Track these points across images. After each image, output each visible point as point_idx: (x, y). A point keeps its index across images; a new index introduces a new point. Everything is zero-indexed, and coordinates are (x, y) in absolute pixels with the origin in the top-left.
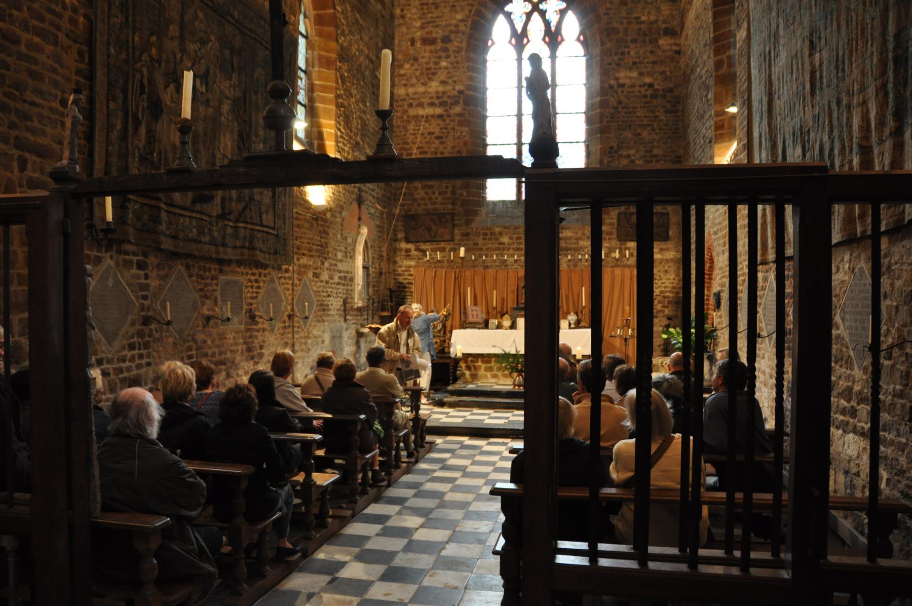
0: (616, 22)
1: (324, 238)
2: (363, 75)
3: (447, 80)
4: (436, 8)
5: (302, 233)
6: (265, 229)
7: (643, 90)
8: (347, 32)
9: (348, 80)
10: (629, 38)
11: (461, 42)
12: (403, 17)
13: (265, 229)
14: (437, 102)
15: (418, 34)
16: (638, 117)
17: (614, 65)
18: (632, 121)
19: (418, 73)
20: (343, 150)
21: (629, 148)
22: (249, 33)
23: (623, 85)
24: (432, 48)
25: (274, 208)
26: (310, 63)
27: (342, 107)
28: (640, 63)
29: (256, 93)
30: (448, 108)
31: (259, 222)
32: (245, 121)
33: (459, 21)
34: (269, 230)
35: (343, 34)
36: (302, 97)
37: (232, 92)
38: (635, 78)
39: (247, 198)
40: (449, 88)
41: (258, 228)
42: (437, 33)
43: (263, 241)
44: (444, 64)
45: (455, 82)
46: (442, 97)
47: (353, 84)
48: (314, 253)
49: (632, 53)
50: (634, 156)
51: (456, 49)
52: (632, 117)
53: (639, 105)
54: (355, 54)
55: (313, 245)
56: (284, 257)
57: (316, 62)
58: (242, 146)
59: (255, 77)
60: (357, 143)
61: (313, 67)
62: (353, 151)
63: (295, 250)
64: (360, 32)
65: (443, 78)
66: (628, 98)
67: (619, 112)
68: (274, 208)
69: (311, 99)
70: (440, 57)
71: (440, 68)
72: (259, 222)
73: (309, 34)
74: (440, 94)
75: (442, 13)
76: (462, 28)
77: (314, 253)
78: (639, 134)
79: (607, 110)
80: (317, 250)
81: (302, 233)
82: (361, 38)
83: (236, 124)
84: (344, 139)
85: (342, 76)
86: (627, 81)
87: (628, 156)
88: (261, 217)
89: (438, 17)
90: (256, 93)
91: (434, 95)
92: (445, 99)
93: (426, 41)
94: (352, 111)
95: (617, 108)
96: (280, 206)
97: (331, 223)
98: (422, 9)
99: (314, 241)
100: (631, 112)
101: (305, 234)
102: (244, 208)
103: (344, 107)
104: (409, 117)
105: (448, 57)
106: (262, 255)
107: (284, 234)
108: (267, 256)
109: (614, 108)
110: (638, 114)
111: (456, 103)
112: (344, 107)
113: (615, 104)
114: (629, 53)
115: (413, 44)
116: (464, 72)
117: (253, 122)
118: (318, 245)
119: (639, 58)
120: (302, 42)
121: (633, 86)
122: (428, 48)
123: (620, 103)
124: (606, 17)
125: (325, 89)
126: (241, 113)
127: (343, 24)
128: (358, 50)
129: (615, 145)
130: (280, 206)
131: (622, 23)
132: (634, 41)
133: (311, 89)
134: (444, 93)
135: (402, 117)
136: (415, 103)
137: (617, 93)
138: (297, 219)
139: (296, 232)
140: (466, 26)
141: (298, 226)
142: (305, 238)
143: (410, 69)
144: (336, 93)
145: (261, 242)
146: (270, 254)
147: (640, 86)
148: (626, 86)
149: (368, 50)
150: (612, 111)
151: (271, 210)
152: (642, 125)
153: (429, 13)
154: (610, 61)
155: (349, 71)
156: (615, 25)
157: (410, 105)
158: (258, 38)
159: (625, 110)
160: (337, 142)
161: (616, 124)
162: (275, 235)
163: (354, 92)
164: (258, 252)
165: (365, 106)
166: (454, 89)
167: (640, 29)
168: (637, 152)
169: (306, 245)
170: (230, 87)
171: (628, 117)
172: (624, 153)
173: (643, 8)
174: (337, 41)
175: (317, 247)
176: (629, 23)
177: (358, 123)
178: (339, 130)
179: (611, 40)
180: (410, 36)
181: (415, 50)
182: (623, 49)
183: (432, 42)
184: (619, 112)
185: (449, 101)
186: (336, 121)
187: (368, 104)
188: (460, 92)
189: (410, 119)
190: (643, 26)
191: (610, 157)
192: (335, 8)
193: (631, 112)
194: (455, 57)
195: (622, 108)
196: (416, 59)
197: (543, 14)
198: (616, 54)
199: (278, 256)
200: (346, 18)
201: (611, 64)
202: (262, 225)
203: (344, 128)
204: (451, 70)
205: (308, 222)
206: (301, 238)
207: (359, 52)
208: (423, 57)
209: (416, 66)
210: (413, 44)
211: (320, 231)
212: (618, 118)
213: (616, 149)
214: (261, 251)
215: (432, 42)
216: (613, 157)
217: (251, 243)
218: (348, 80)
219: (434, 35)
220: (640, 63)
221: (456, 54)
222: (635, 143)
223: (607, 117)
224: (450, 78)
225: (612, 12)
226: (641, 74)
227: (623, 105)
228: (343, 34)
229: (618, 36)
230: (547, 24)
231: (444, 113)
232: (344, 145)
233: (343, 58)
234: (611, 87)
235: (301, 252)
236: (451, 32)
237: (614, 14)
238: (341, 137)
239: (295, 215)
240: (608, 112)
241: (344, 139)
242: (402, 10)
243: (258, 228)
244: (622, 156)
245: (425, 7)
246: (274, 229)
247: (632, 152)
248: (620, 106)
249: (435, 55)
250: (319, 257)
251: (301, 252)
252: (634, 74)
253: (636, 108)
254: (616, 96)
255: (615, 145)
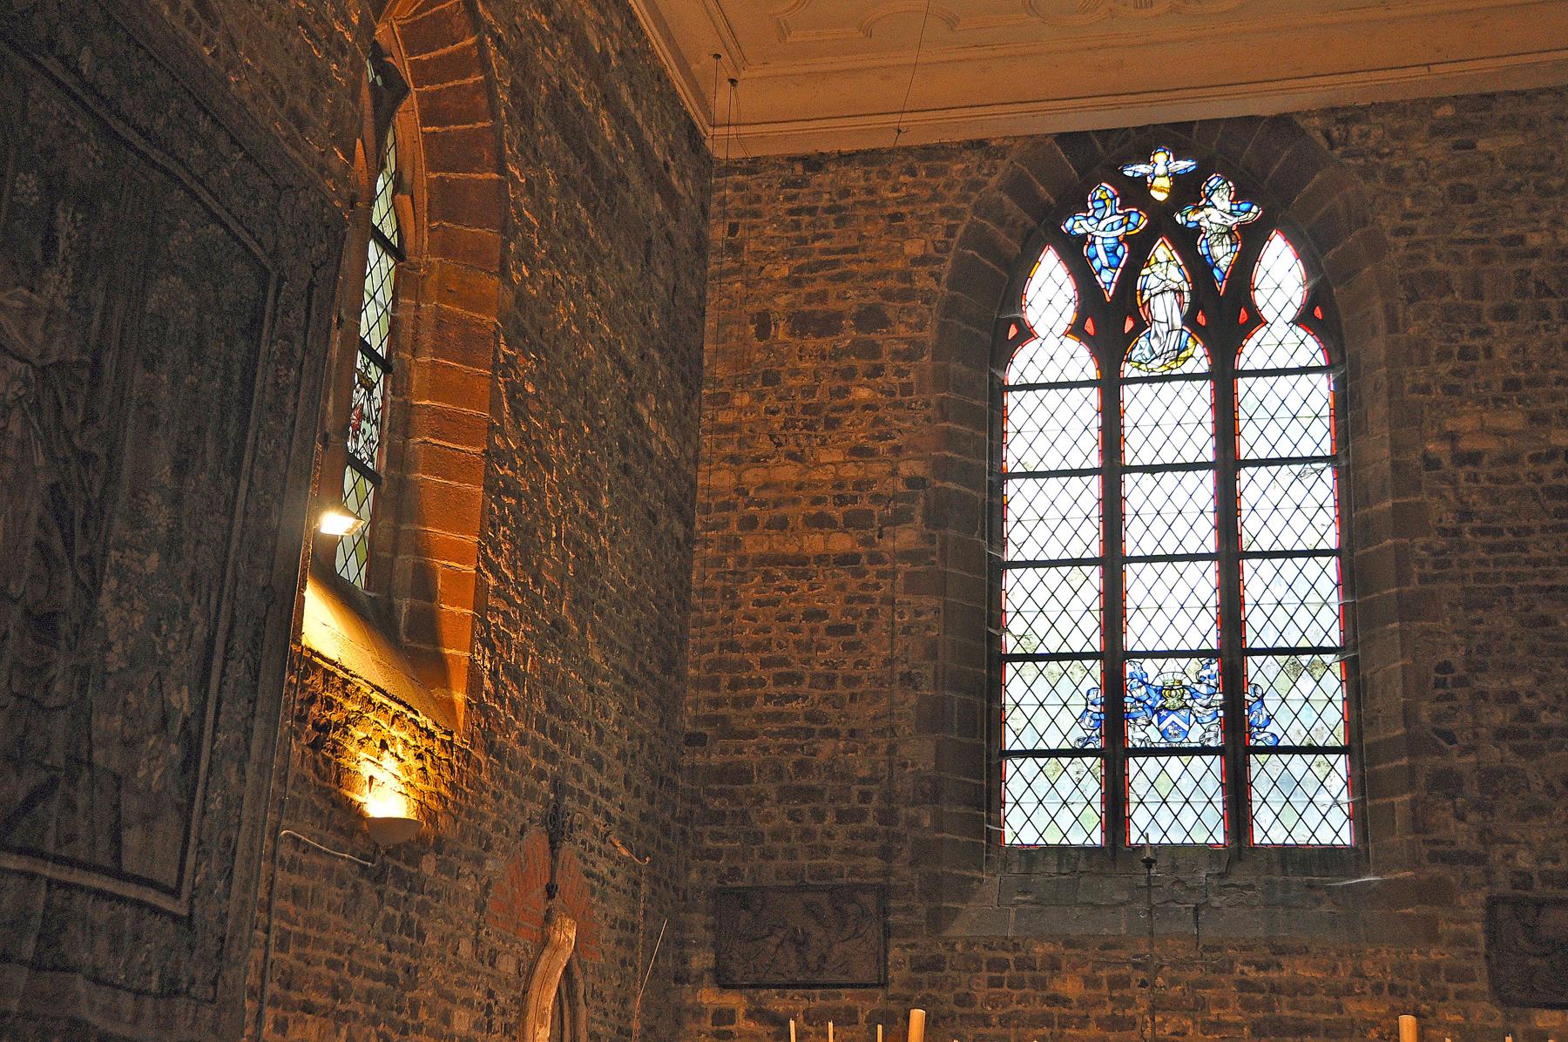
0: (1439, 257)
1: (402, 948)
2: (591, 405)
3: (870, 444)
4: (841, 222)
5: (309, 922)
6: (132, 891)
7: (1547, 470)
8: (541, 254)
9: (535, 407)
10: (1487, 305)
11: (920, 327)
12: (734, 249)
13: (132, 891)
14: (837, 513)
15: (782, 301)
16: (1535, 563)
17: (1437, 391)
18: (1512, 577)
19: (777, 423)
20: (504, 638)
21: (1511, 668)
22: (140, 144)
23: (1474, 458)
24: (826, 343)
25: (185, 811)
26: (407, 330)
27: (507, 491)
28: (1531, 382)
29: (149, 365)
30: (872, 533)
31: (104, 860)
32: (86, 458)
33: (916, 261)
34: (150, 896)
35: (526, 255)
36: (365, 442)
37: (39, 336)
38: (1517, 433)
39: (58, 757)
40: (878, 469)
41: (95, 881)
42: (842, 297)
43: (116, 940)
44: (864, 394)
45: (897, 450)
46: (854, 500)
47: (555, 426)
48: (358, 1007)
49: (1501, 353)
50: (1530, 695)
51: (902, 346)
52: (1513, 562)
53: (1534, 523)
54: (566, 330)
55: (354, 970)
56: (208, 1012)
57: (427, 337)
58: (57, 544)
59: (152, 304)
60: (558, 625)
61: (414, 352)
62: (542, 650)
63: (273, 988)
64: (589, 264)
65: (860, 437)
66: (1496, 501)
67: (1464, 547)
68: (185, 811)
69: (398, 457)
70: (849, 373)
71: (851, 408)
72: (104, 860)
73: (410, 244)
74: (849, 491)
75: (861, 237)
76: (923, 282)
77: (358, 1007)
78: (1545, 621)
79: (1420, 541)
80: (370, 994)
81: (309, 922)
82: (592, 286)
83: (40, 461)
84: (511, 602)
85: (514, 390)
86: (1491, 444)
87: (1511, 697)
88: (117, 840)
89: (845, 251)
90: (149, 365)
91: (828, 491)
92: (864, 504)
93: (801, 323)
94: (546, 516)
95: (1456, 532)
96: (216, 805)
97: (437, 895)
98: (797, 226)
99: (356, 958)
100: (1508, 547)
101: (323, 927)
102: (36, 797)
103: (518, 496)
104: (742, 561)
105: (877, 371)
106: (103, 996)
107: (222, 920)
108: (127, 1002)
109: (1444, 532)
110: (1535, 552)
111: (901, 518)
112: (518, 496)
113: (1449, 521)
114: (1489, 352)
115: (763, 331)
116: (928, 419)
117: (126, 474)
118: (375, 976)
119: (1528, 365)
120: (379, 268)
121: (1512, 459)
122: (811, 343)
123: (1466, 515)
124: (1402, 241)
125: (448, 425)
126: (72, 420)
127: (531, 227)
128: (577, 318)
129: (1457, 657)
130: (216, 805)
131: (1459, 258)
132: (1506, 313)
133: (400, 422)
134: (859, 485)
135: (720, 561)
136: (764, 516)
137: (1454, 483)
138: (293, 866)
139: (283, 915)
140: (936, 276)
141: (296, 895)
142: (324, 945)
143: (751, 408)
144: (490, 441)
145: (102, 943)
146: (139, 993)
147: (1535, 459)
148: (1486, 459)
149: (614, 330)
150: (1441, 543)
151: (173, 817)
152: (1552, 588)
153: (817, 238)
154: (1422, 381)
155: (542, 380)
156: (1435, 265)
157: (750, 523)
158: (180, 172)
159: (1488, 540)
160: (481, 607)
161: (1457, 587)
162: (176, 918)
163: (556, 451)
164: (80, 985)
165: (594, 505)
166: (894, 473)
167: (1524, 275)
168: (1540, 681)
169: (323, 969)
170: (30, 311)
171: (1497, 563)
172: (1492, 684)
173: (1534, 208)
174: (504, 272)
175: (368, 983)
176: (1487, 257)
177: (564, 558)
178: (494, 569)
179: (1423, 314)
180: (756, 307)
181: (770, 349)
182: (1466, 341)
183: (828, 324)
184: (1464, 547)
185: (876, 510)
186: (482, 535)
187: (605, 502)
188: (912, 482)
189: (748, 567)
190: (1535, 263)
191: (1439, 699)
192: (502, 169)
193: (1508, 547)
194: (900, 373)
195: (1473, 531)
196: (771, 379)
197: (1186, 241)
198: (1444, 355)
199: (180, 1004)
200: (542, 208)
201: (1426, 390)
202: (120, 875)
203: (512, 566)
204: (887, 414)
205: (341, 884)
206: (303, 940)
207: (582, 329)
208: (795, 373)
209: (771, 401)
210: (763, 331)
211: (389, 921)
212: (1464, 564)
213: (1461, 671)
214: (97, 980)
215: (828, 324)
216: (1450, 697)
217: (47, 939)
218: (535, 407)
219: (833, 305)
220: (1531, 382)
221: (904, 365)
222: (1533, 650)
223: (1422, 563)
224: (882, 437)
225: (1422, 224)
226: (1538, 419)
227: (1477, 523)
228: (526, 255)
229: (1447, 299)
230: (1198, 267)
231: (860, 549)
232: (508, 620)
233: (521, 333)
234: (1431, 463)
235: (295, 996)
236: (887, 295)
237: (1428, 231)
238: (498, 593)
239: (285, 851)
240: (1426, 548)
241: (511, 602)
242: (733, 229)
243: (95, 881)
244: (1483, 695)
245: (806, 219)
246: (175, 893)
247: (1522, 682)
248: (1466, 527)
249: (834, 365)
250: (375, 1021)
251: (295, 996)
252: (1513, 420)
253: (1529, 531)
254: (1451, 496)
255: (1457, 657)
